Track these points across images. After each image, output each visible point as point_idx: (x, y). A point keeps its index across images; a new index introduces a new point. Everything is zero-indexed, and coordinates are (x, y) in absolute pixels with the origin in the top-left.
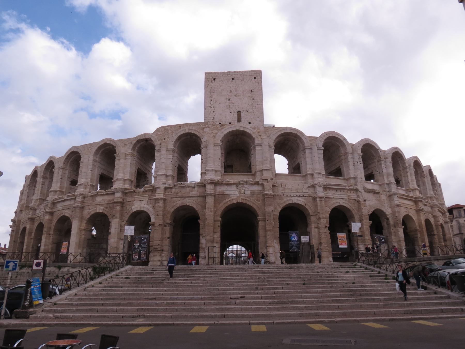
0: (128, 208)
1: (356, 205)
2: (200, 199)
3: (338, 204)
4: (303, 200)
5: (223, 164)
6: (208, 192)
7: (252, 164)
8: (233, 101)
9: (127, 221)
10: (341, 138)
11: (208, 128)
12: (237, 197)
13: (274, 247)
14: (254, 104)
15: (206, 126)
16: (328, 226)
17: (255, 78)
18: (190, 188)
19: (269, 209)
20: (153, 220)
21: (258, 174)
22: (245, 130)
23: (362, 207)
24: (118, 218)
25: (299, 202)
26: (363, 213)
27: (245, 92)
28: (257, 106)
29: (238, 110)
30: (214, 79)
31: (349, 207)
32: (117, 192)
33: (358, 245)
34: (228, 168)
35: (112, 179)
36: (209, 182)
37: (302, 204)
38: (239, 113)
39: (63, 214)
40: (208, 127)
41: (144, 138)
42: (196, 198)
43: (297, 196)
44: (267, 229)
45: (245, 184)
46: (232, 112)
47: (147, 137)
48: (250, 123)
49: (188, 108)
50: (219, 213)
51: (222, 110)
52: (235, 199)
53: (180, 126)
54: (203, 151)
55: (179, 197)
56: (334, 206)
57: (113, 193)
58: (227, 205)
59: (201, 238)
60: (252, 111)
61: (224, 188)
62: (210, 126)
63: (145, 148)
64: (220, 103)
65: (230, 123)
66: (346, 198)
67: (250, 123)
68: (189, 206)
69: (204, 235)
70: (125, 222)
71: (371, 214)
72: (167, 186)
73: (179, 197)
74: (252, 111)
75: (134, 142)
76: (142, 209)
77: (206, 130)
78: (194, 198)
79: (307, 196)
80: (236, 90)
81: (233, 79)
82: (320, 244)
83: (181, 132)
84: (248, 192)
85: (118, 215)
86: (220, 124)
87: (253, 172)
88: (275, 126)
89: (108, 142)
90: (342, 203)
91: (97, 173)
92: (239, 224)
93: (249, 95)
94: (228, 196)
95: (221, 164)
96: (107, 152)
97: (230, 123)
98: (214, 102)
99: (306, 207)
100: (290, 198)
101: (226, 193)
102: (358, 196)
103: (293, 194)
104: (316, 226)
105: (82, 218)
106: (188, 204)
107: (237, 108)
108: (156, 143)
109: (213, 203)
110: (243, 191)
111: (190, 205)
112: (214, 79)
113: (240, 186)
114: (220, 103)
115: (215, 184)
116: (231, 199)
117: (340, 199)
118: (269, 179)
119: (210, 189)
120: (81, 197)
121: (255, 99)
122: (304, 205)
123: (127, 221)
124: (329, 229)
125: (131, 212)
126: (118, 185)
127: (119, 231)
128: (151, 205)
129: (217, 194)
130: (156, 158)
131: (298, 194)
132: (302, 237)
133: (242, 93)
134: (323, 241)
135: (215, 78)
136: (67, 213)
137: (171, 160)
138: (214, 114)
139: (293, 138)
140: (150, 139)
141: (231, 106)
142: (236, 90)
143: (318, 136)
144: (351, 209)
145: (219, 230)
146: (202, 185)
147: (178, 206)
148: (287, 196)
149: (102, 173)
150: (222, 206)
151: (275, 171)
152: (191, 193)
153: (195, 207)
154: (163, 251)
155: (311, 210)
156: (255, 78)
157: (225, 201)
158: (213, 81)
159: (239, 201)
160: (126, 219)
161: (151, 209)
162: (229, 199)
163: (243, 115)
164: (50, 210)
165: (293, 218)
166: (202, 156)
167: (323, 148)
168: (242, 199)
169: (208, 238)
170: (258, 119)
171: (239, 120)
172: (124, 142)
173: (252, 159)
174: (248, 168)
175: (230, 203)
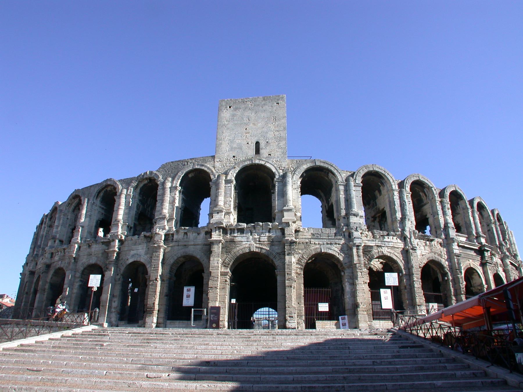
6: (215, 239)
9: (122, 275)
16: (369, 281)
18: (194, 234)
38: (257, 144)
44: (287, 284)
71: (424, 266)
104: (351, 281)
119: (216, 236)
123: (122, 275)
128: (148, 255)
134: (359, 300)
160: (122, 272)
162: (241, 247)
167: (362, 185)
171: (258, 151)
175: (241, 252)
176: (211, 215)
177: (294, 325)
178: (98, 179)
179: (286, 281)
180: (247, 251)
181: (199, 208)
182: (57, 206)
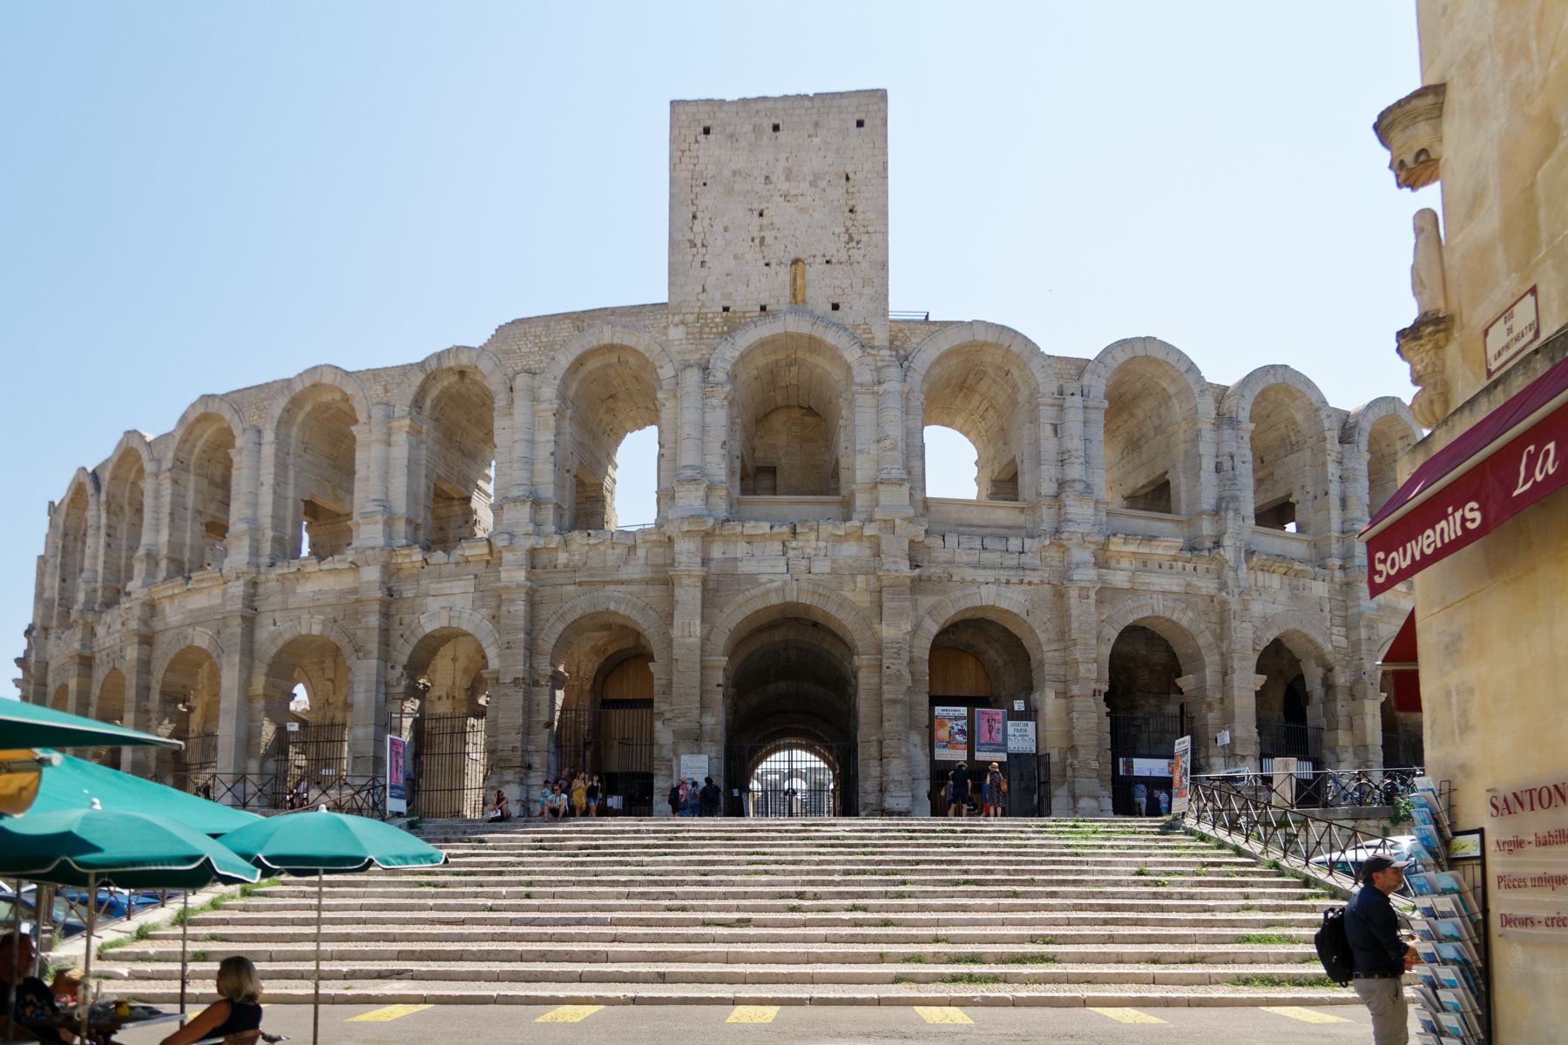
0: (407, 619)
2: (654, 593)
5: (738, 464)
7: (843, 463)
8: (775, 220)
11: (681, 328)
12: (785, 583)
13: (909, 759)
14: (852, 230)
15: (677, 319)
16: (1106, 688)
19: (890, 631)
20: (494, 663)
21: (861, 500)
23: (1234, 624)
24: (375, 654)
25: (1004, 605)
26: (1238, 647)
27: (823, 184)
28: (865, 238)
29: (792, 256)
31: (1184, 622)
32: (367, 564)
33: (1208, 757)
34: (757, 476)
35: (349, 516)
39: (188, 642)
40: (682, 322)
43: (997, 582)
44: (886, 696)
45: (813, 536)
46: (773, 266)
47: (464, 360)
48: (835, 307)
49: (611, 252)
50: (721, 640)
51: (736, 257)
52: (776, 590)
53: (580, 320)
54: (666, 415)
55: (580, 584)
56: (1130, 620)
57: (355, 566)
58: (748, 611)
59: (658, 725)
60: (844, 258)
62: (690, 318)
63: (453, 404)
64: (726, 230)
66: (1177, 589)
68: (615, 613)
69: (668, 715)
70: (399, 670)
73: (580, 584)
74: (844, 258)
75: (419, 378)
76: (455, 625)
79: (1036, 580)
81: (776, 128)
82: (1073, 749)
84: (822, 566)
85: (373, 646)
86: (726, 309)
87: (844, 492)
88: (931, 318)
92: (792, 685)
93: (837, 193)
94: (752, 579)
95: (731, 462)
96: (320, 419)
97: (763, 308)
98: (706, 222)
99: (1029, 620)
100: (974, 589)
101: (746, 567)
104: (1060, 687)
106: (612, 607)
107: (790, 246)
108: (495, 383)
109: (698, 603)
110: (804, 562)
111: (621, 612)
112: (707, 131)
113: (794, 544)
116: (762, 588)
118: (898, 522)
121: (858, 208)
122: (1023, 615)
123: (405, 667)
124: (1109, 698)
126: (368, 534)
128: (484, 611)
129: (713, 570)
130: (497, 440)
133: (813, 184)
135: (708, 123)
136: (201, 639)
138: (704, 272)
141: (768, 241)
143: (1091, 354)
145: (718, 697)
146: (662, 537)
147: (578, 613)
148: (963, 581)
151: (924, 489)
152: (623, 569)
154: (529, 767)
155: (1046, 631)
156: (860, 124)
157: (740, 599)
158: (702, 138)
159: (791, 596)
160: (404, 659)
163: (814, 272)
164: (144, 629)
165: (979, 659)
166: (660, 432)
167: (1106, 404)
169: (681, 724)
170: (868, 291)
173: (842, 444)
174: (823, 480)
175: (760, 605)
176: (665, 496)
177: (903, 803)
178: (282, 362)
179: (885, 687)
180: (775, 600)
181: (610, 458)
182: (135, 443)
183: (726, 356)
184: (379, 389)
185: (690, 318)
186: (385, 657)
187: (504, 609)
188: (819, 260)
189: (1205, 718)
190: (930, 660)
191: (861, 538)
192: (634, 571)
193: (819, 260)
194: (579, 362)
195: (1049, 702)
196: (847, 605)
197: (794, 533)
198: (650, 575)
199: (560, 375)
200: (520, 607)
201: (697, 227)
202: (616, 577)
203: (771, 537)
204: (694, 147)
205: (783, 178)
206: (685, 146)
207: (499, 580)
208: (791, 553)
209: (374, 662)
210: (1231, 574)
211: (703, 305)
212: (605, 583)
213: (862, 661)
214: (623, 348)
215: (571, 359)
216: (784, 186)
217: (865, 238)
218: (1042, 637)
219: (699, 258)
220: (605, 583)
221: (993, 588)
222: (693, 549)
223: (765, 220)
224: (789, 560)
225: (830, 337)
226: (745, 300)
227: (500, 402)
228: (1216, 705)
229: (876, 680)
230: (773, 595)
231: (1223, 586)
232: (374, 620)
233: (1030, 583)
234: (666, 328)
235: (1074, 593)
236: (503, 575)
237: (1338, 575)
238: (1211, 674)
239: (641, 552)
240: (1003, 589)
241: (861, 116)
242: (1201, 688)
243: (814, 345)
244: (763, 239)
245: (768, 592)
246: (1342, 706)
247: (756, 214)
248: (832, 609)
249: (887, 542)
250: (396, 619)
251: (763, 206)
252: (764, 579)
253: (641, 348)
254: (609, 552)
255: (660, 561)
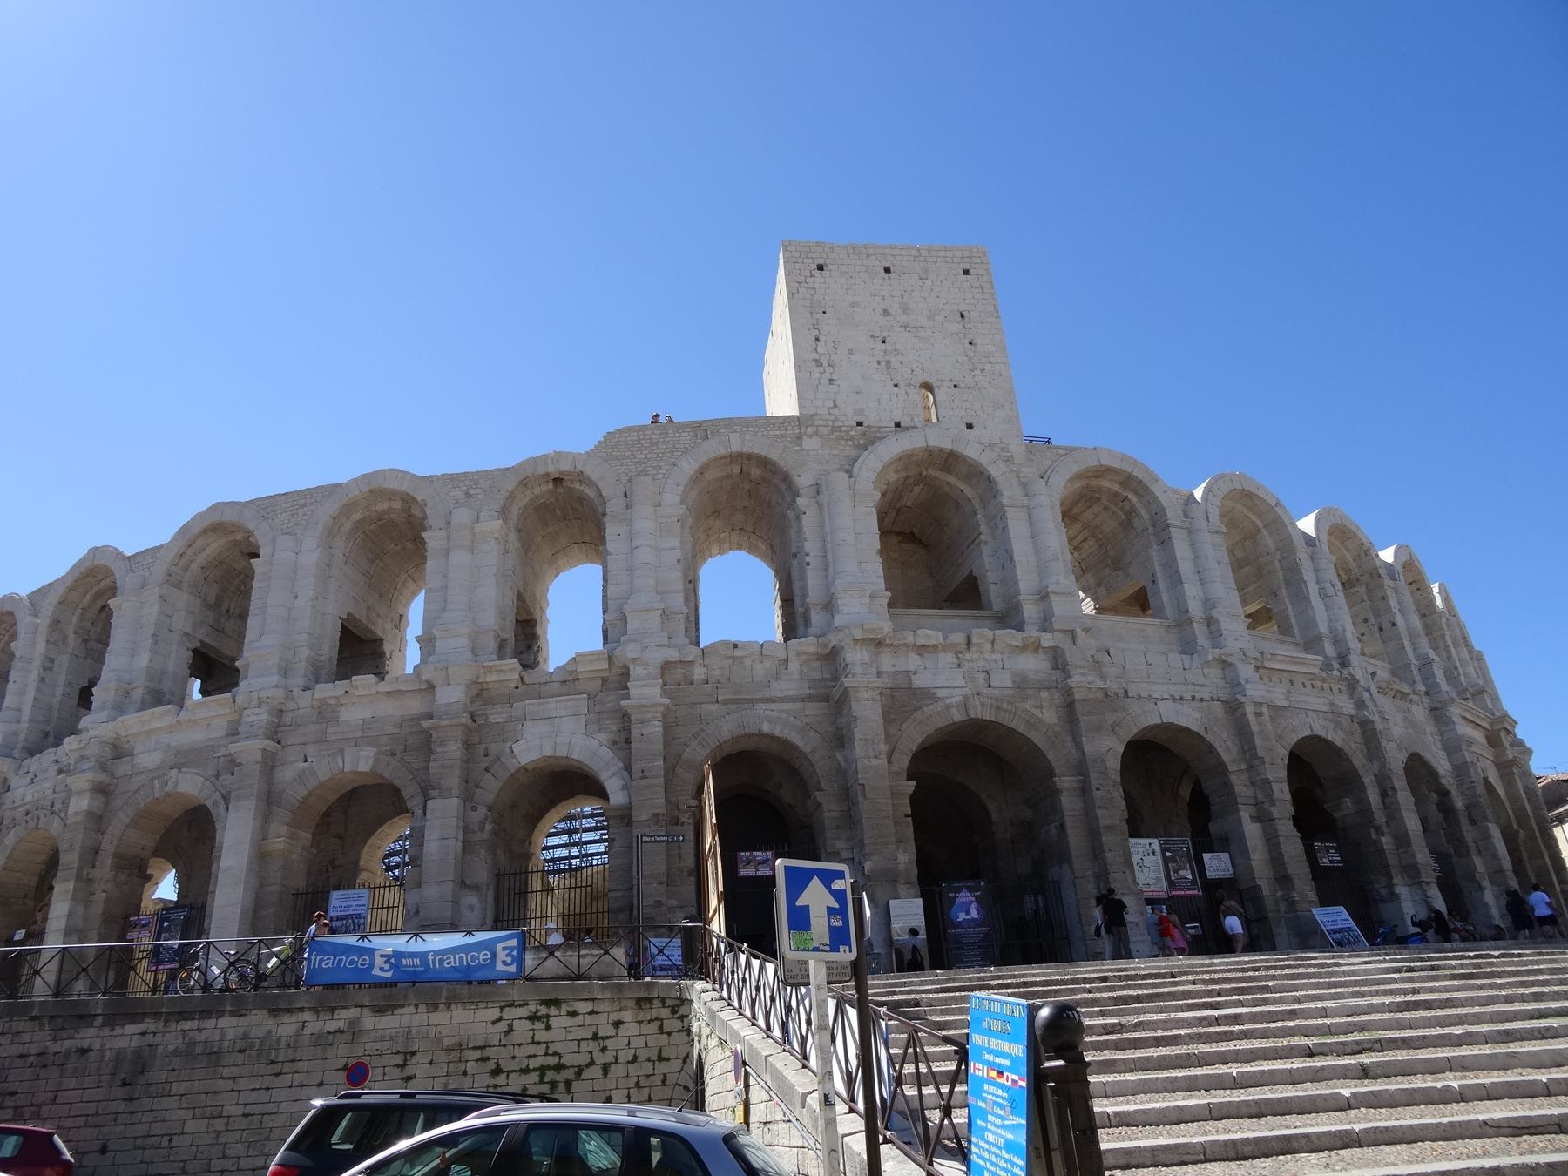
0: (494, 749)
1: (1359, 738)
2: (814, 710)
3: (1307, 733)
4: (1197, 715)
10: (1268, 499)
11: (815, 439)
15: (810, 430)
17: (966, 272)
21: (1029, 611)
22: (959, 448)
24: (456, 792)
27: (939, 319)
28: (988, 367)
30: (820, 268)
31: (1338, 743)
36: (858, 634)
37: (1194, 728)
40: (816, 434)
41: (551, 469)
42: (798, 705)
43: (1173, 699)
44: (1103, 822)
45: (988, 646)
47: (565, 466)
48: (970, 427)
50: (903, 762)
53: (702, 430)
55: (726, 702)
61: (913, 661)
65: (898, 425)
66: (1325, 708)
67: (970, 427)
70: (482, 811)
72: (673, 655)
75: (510, 484)
77: (810, 444)
78: (786, 706)
79: (1207, 696)
80: (906, 310)
83: (713, 448)
84: (1003, 680)
85: (453, 781)
86: (860, 424)
89: (392, 485)
90: (1321, 728)
91: (334, 611)
93: (955, 326)
94: (927, 695)
97: (898, 425)
99: (1208, 737)
101: (920, 681)
102: (1360, 705)
103: (1160, 690)
105: (270, 801)
106: (766, 728)
107: (918, 371)
108: (610, 489)
111: (777, 733)
113: (968, 656)
114: (851, 352)
115: (878, 643)
117: (1314, 712)
118: (1079, 631)
120: (264, 708)
122: (1202, 733)
125: (513, 765)
127: (459, 850)
128: (602, 737)
131: (1177, 691)
132: (1206, 856)
133: (931, 318)
135: (821, 261)
137: (677, 554)
138: (834, 388)
139: (1116, 487)
140: (582, 478)
142: (906, 310)
144: (1346, 749)
147: (726, 735)
149: (349, 614)
150: (914, 736)
153: (795, 738)
159: (978, 711)
161: (606, 753)
168: (983, 704)
172: (466, 485)
180: (958, 716)
183: (873, 464)
184: (460, 495)
185: (825, 431)
186: (468, 799)
187: (635, 732)
188: (946, 384)
189: (1377, 843)
190: (1122, 783)
191: (1037, 647)
192: (791, 684)
193: (946, 384)
194: (702, 471)
195: (1252, 831)
196: (1038, 719)
197: (969, 643)
198: (807, 691)
199: (684, 481)
200: (656, 728)
201: (821, 347)
202: (767, 694)
203: (945, 648)
204: (810, 280)
205: (900, 312)
206: (801, 279)
207: (627, 697)
208: (966, 666)
209: (455, 802)
210: (1366, 695)
211: (836, 419)
212: (752, 701)
213: (1065, 782)
214: (750, 457)
215: (696, 466)
216: (904, 318)
217: (988, 367)
218: (1226, 757)
219: (827, 376)
220: (752, 701)
221: (1169, 703)
222: (867, 660)
223: (887, 346)
224: (961, 672)
225: (972, 452)
226: (879, 413)
227: (614, 506)
228: (1385, 830)
229: (1080, 804)
230: (954, 711)
231: (1360, 705)
232: (454, 750)
233: (1202, 700)
234: (799, 438)
235: (1249, 709)
236: (633, 692)
237: (1426, 700)
238: (1373, 796)
239: (794, 666)
240: (1178, 706)
241: (967, 267)
242: (1364, 810)
243: (949, 460)
244: (888, 362)
245: (948, 707)
246: (1469, 832)
247: (879, 341)
248: (1018, 725)
249: (1072, 655)
250: (480, 749)
251: (885, 334)
252: (941, 693)
253: (774, 455)
254: (758, 666)
255: (817, 675)
